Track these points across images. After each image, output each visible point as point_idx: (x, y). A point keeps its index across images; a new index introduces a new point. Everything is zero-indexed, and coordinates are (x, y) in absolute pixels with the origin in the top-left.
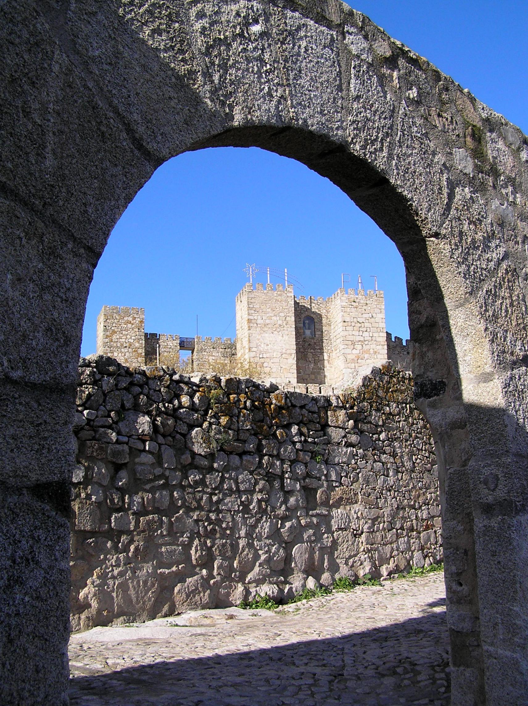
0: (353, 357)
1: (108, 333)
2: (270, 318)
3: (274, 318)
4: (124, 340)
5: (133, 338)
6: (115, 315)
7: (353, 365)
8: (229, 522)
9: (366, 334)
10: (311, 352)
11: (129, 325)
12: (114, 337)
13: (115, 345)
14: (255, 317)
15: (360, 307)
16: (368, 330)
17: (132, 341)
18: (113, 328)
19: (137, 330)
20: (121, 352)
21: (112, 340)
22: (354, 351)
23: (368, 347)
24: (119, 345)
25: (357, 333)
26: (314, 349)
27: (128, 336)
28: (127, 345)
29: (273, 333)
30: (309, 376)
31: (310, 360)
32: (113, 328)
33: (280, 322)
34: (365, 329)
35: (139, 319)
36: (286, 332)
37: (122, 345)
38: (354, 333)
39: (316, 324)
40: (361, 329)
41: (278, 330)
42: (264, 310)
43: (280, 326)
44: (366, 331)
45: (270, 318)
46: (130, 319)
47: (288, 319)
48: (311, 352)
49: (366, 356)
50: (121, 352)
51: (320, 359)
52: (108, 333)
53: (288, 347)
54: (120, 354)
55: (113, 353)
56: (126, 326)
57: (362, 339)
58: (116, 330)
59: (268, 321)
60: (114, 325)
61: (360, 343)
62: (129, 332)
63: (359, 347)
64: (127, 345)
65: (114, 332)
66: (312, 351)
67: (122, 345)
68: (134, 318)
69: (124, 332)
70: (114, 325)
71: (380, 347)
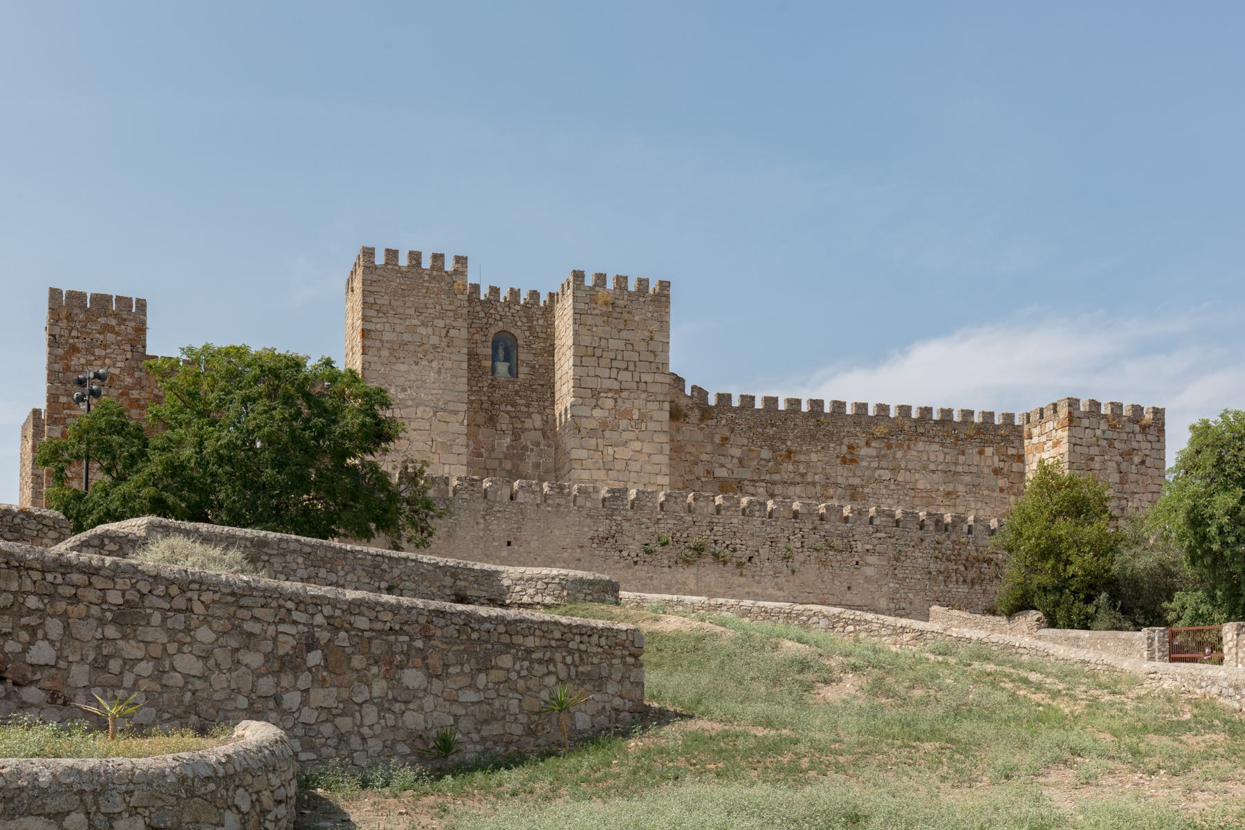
0: (593, 424)
2: (412, 330)
3: (422, 330)
5: (119, 364)
7: (593, 442)
9: (625, 376)
10: (508, 412)
11: (111, 337)
14: (379, 327)
15: (615, 315)
16: (632, 367)
17: (117, 371)
19: (128, 348)
22: (597, 413)
23: (628, 405)
25: (606, 373)
26: (514, 405)
27: (107, 361)
29: (416, 363)
30: (501, 463)
31: (504, 427)
33: (435, 340)
34: (623, 365)
35: (133, 324)
36: (448, 364)
39: (520, 350)
40: (615, 364)
42: (400, 310)
43: (435, 347)
44: (626, 369)
45: (412, 330)
46: (113, 322)
47: (453, 333)
48: (508, 412)
49: (623, 423)
51: (526, 426)
52: (60, 351)
53: (448, 398)
56: (101, 337)
57: (616, 386)
58: (80, 346)
59: (407, 337)
60: (74, 333)
61: (610, 395)
62: (109, 351)
63: (609, 403)
65: (74, 349)
66: (509, 408)
68: (122, 321)
69: (98, 352)
70: (74, 333)
71: (655, 406)
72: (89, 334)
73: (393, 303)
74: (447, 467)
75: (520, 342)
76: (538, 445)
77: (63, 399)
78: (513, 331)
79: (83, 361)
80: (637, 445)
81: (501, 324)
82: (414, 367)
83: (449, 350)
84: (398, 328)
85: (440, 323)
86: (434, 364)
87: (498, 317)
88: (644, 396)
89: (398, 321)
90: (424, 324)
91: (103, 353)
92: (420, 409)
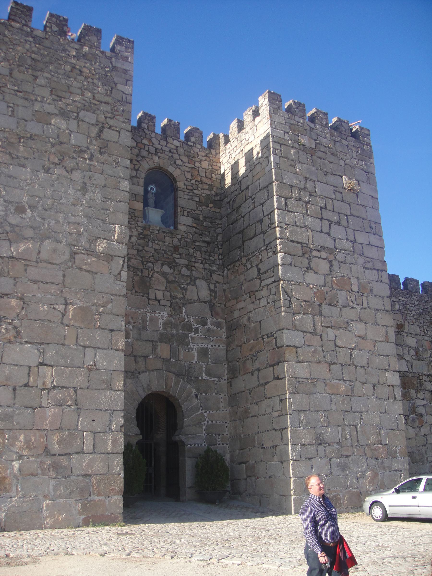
2: (43, 118)
10: (164, 274)
15: (319, 154)
16: (344, 222)
22: (310, 277)
23: (344, 270)
25: (316, 224)
29: (47, 171)
30: (155, 348)
31: (160, 295)
34: (335, 218)
36: (99, 179)
38: (309, 221)
39: (180, 194)
40: (326, 214)
41: (70, 164)
42: (28, 88)
43: (80, 151)
44: (338, 223)
47: (108, 134)
48: (164, 274)
51: (188, 296)
57: (329, 243)
59: (34, 128)
61: (324, 255)
63: (324, 266)
66: (166, 269)
73: (16, 73)
74: (90, 352)
75: (180, 184)
76: (204, 323)
78: (171, 169)
80: (358, 328)
81: (156, 159)
82: (42, 175)
83: (103, 158)
84: (21, 112)
85: (89, 117)
86: (77, 175)
87: (153, 150)
88: (361, 261)
89: (20, 102)
90: (63, 114)
92: (48, 245)
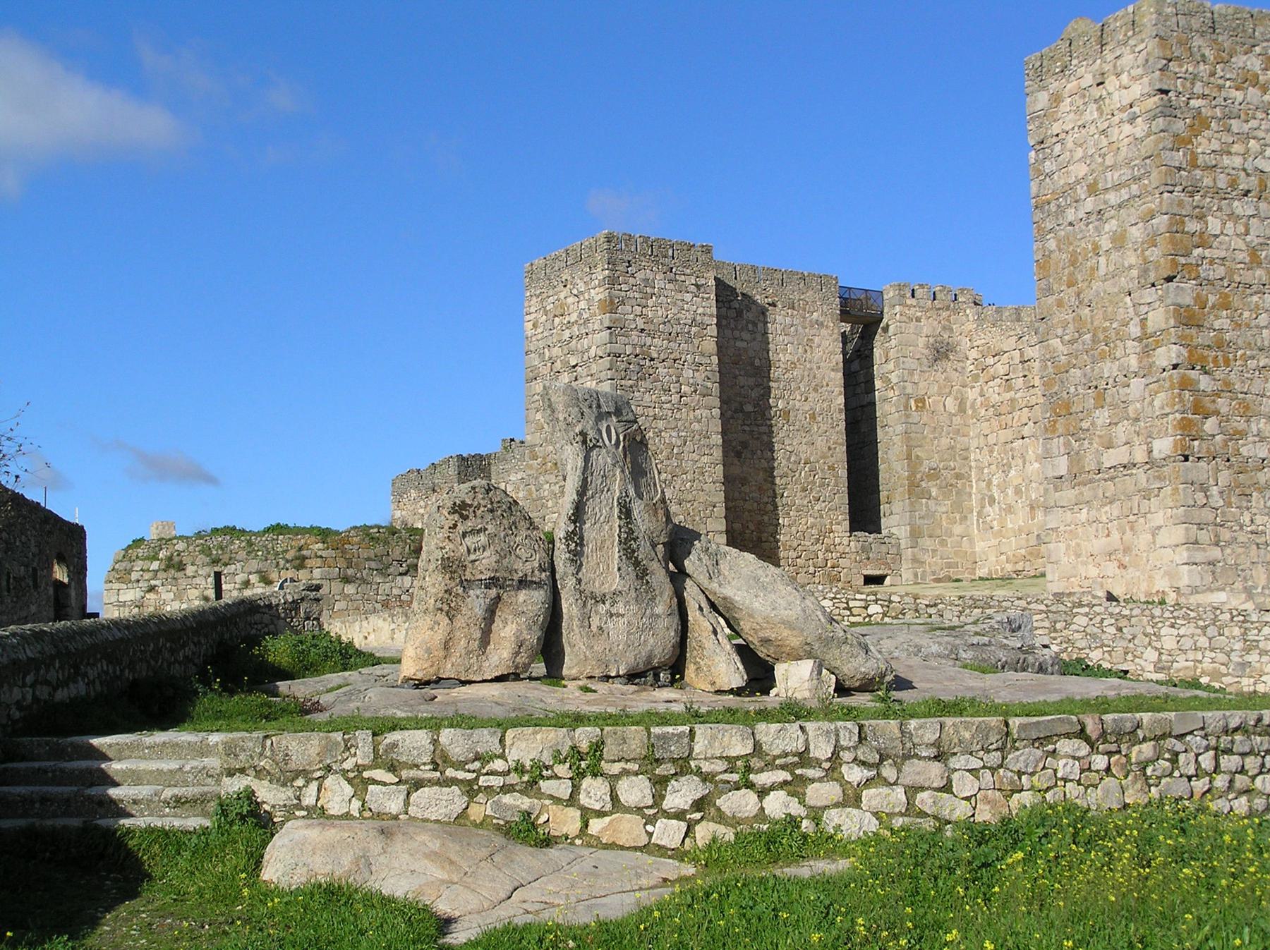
1: (1179, 126)
4: (1237, 161)
6: (1197, 42)
8: (502, 756)
12: (1205, 145)
13: (1207, 181)
18: (1194, 103)
20: (1232, 216)
21: (1194, 156)
24: (1222, 182)
28: (1253, 182)
32: (1194, 103)
37: (1233, 184)
50: (1232, 216)
52: (1179, 126)
54: (1230, 225)
55: (1201, 218)
56: (1239, 95)
60: (1198, 88)
64: (1253, 182)
65: (1200, 123)
67: (1233, 184)
70: (1198, 88)
72: (1220, 87)
77: (1192, 226)
79: (1215, 145)
91: (1246, 127)
